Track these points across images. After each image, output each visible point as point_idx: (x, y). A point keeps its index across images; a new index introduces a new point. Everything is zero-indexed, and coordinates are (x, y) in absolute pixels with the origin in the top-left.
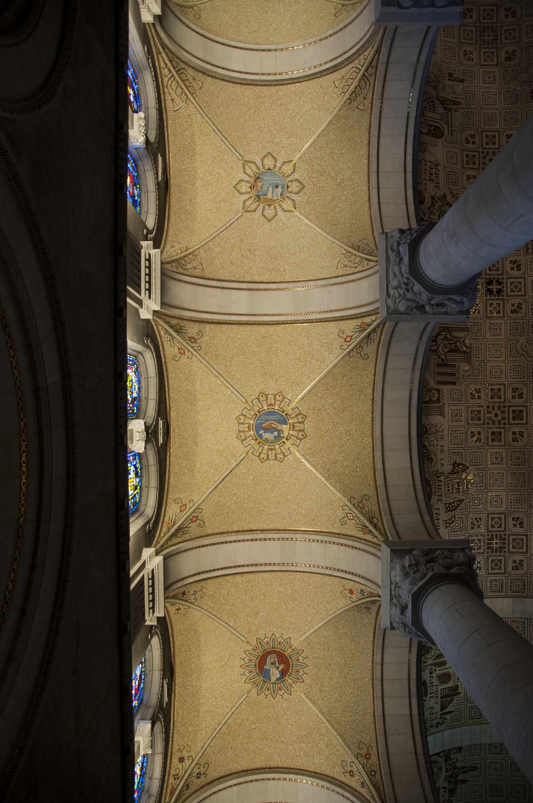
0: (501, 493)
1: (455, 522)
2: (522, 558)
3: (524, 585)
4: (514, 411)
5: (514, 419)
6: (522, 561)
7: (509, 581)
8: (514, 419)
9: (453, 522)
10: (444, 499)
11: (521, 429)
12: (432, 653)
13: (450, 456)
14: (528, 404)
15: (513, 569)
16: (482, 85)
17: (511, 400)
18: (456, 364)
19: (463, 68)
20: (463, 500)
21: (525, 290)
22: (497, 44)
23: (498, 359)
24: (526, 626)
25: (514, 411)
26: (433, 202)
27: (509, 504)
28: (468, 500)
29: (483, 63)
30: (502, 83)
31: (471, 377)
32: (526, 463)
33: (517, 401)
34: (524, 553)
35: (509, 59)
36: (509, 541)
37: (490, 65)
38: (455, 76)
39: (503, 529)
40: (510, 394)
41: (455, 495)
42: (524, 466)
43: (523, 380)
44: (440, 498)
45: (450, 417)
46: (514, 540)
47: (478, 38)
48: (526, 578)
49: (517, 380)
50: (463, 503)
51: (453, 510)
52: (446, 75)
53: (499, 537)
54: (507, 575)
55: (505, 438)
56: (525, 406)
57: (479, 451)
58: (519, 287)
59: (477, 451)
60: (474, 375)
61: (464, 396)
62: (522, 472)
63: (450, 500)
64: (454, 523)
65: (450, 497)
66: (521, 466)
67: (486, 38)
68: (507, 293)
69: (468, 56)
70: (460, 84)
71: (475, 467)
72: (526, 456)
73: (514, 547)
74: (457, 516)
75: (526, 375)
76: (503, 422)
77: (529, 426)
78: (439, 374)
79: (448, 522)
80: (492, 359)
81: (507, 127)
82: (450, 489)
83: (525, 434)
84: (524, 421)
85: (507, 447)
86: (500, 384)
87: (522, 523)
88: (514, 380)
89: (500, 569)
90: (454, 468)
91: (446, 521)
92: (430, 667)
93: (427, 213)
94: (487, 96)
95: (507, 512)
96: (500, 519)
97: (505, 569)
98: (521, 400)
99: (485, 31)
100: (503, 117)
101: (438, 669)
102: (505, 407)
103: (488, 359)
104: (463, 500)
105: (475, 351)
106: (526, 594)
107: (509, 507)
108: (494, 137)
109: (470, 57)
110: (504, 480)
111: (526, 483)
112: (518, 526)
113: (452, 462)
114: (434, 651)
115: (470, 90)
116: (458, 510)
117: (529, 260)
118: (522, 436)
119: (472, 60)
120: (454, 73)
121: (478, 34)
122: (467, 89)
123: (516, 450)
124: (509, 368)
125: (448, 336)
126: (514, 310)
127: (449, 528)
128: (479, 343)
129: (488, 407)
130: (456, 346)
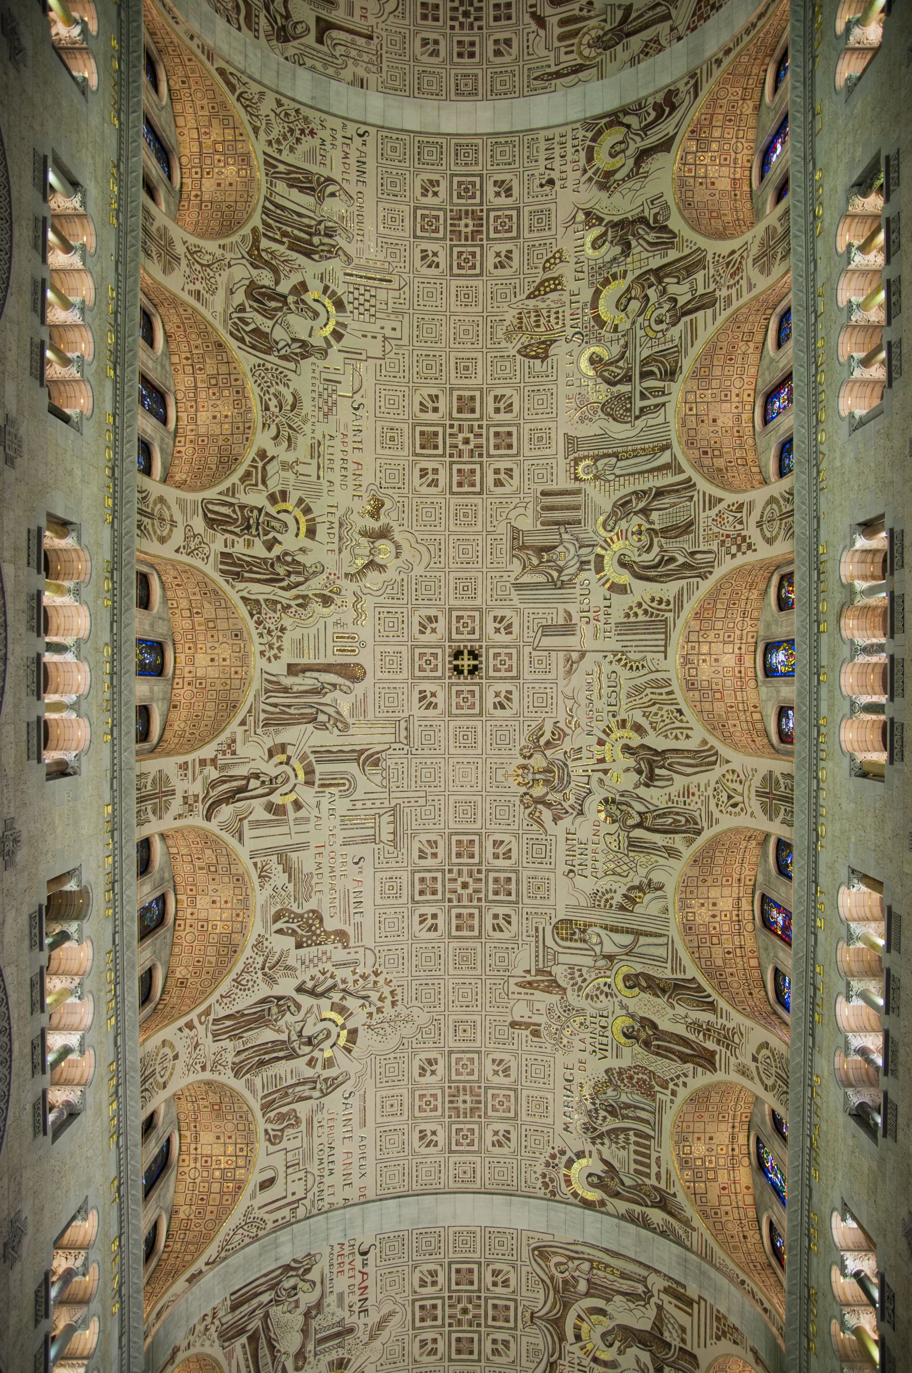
0: (459, 309)
1: (543, 261)
2: (424, 200)
3: (419, 153)
4: (436, 447)
5: (436, 434)
6: (423, 195)
7: (444, 162)
8: (436, 434)
9: (548, 261)
10: (566, 297)
11: (424, 416)
12: (587, 37)
13: (555, 370)
14: (411, 458)
15: (438, 182)
16: (478, 1018)
17: (440, 467)
18: (539, 527)
19: (511, 1047)
20: (528, 298)
21: (413, 655)
22: (450, 1087)
23: (461, 537)
24: (416, 86)
25: (436, 447)
26: (581, 805)
27: (444, 290)
28: (519, 298)
29: (476, 1056)
30: (442, 1022)
31: (512, 506)
32: (415, 358)
33: (430, 465)
34: (421, 208)
35: (430, 1062)
36: (445, 228)
37: (463, 1052)
38: (528, 1032)
39: (456, 250)
40: (442, 477)
41: (543, 305)
42: (419, 352)
43: (419, 500)
44: (574, 299)
45: (553, 436)
46: (437, 230)
47: (482, 1098)
48: (417, 166)
49: (429, 501)
50: (527, 293)
51: (548, 280)
52: (544, 1033)
53: (463, 235)
54: (449, 172)
55: (451, 402)
56: (417, 455)
57: (497, 381)
58: (423, 662)
59: (502, 381)
60: (507, 510)
61: (526, 472)
62: (423, 344)
63: (554, 296)
64: (545, 258)
65: (553, 301)
66: (424, 353)
67: (468, 1098)
68: (444, 652)
69: (501, 1068)
70: (517, 1019)
71: (506, 354)
72: (416, 369)
73: (437, 218)
74: (540, 270)
75: (415, 508)
76: (455, 430)
77: (411, 421)
78: (576, 508)
79: (558, 261)
80: (472, 538)
81: (436, 945)
82: (553, 316)
83: (417, 407)
84: (418, 429)
85: (448, 386)
86: (459, 493)
87: (423, 258)
88: (435, 501)
89: (460, 184)
90: (546, 351)
91: (561, 261)
92: (592, 13)
93: (594, 785)
94: (469, 999)
95: (448, 278)
96: (460, 267)
97: (451, 182)
98: (424, 465)
99: (471, 1109)
100: (442, 961)
101: (577, 12)
102: (451, 456)
103: (480, 537)
104: (528, 298)
105: (504, 552)
106: (417, 139)
107: (444, 286)
108: (458, 928)
109: (498, 1065)
110: (452, 331)
111: (415, 324)
112: (430, 254)
113: (549, 360)
114: (585, 41)
115: (500, 1010)
116: (538, 280)
117: (405, 708)
118: (421, 404)
119: (494, 1061)
120: (530, 1037)
121: (482, 1106)
122: (504, 1010)
123: (434, 381)
124: (443, 521)
125: (555, 574)
126: (431, 622)
127: (555, 250)
128: (495, 565)
129: (481, 455)
130: (540, 558)
